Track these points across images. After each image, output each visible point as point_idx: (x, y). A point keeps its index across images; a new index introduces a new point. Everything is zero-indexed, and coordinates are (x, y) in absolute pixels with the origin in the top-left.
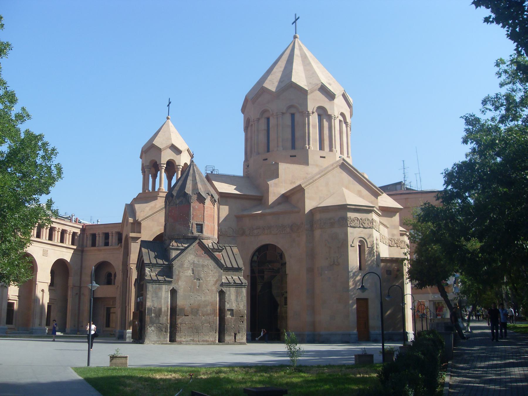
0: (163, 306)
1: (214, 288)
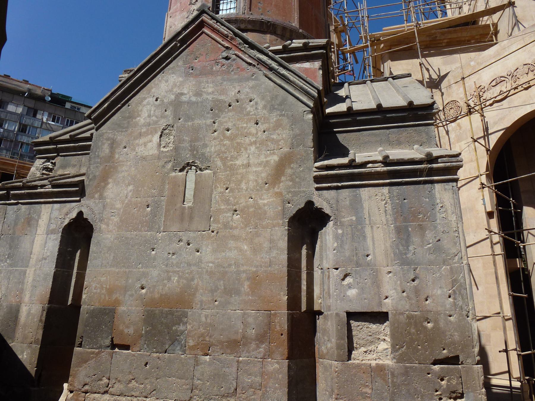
0: (26, 299)
1: (268, 200)
